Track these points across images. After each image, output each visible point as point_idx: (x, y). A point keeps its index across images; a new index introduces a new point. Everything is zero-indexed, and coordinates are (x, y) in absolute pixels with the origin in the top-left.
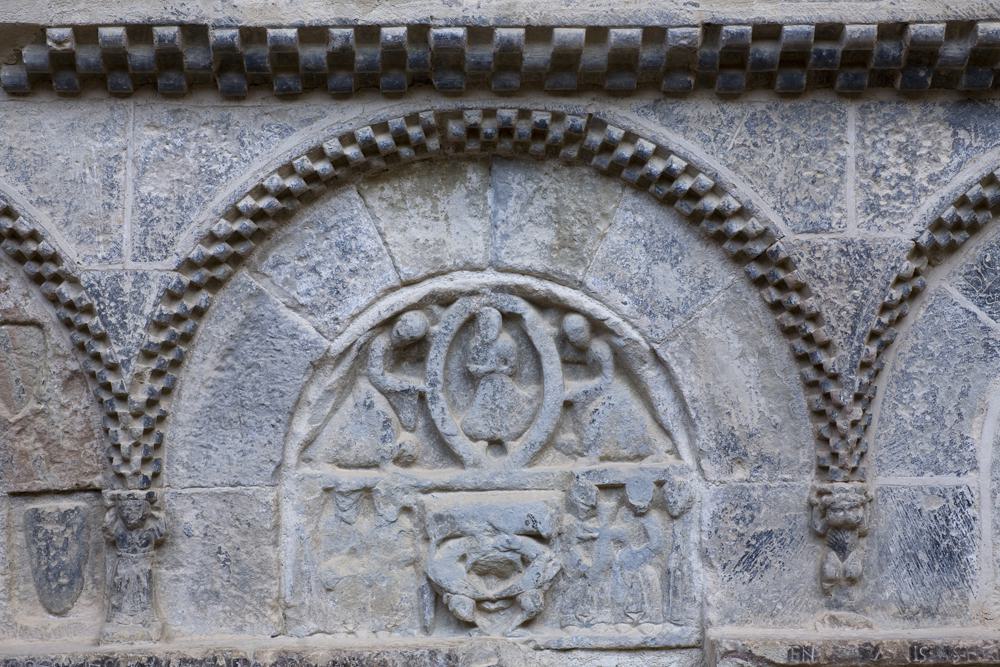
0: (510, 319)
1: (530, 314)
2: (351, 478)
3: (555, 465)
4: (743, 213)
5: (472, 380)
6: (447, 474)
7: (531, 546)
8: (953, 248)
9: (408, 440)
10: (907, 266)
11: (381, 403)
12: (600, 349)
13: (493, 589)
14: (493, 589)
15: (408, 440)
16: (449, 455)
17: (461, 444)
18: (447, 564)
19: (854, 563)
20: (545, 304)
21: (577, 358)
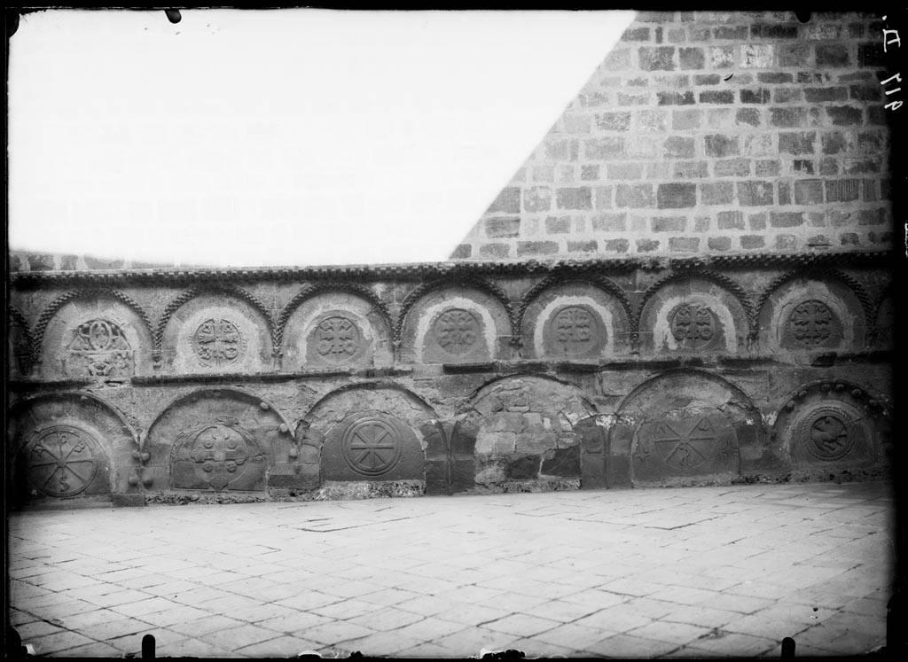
0: (103, 325)
1: (106, 325)
2: (76, 352)
3: (111, 351)
4: (137, 305)
5: (97, 336)
6: (93, 352)
7: (106, 364)
8: (174, 310)
9: (87, 346)
10: (165, 313)
11: (82, 339)
12: (118, 331)
13: (100, 371)
14: (100, 371)
15: (87, 346)
16: (94, 349)
17: (95, 347)
18: (91, 367)
19: (158, 364)
20: (109, 323)
21: (115, 333)
